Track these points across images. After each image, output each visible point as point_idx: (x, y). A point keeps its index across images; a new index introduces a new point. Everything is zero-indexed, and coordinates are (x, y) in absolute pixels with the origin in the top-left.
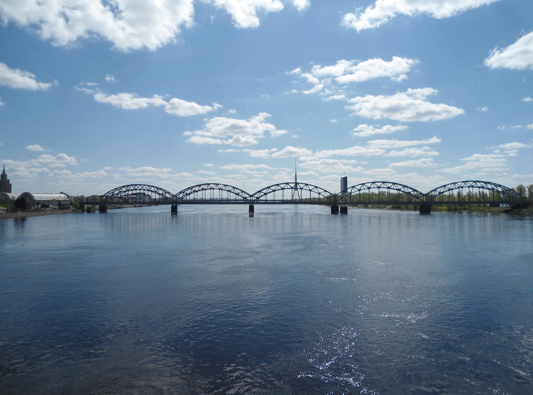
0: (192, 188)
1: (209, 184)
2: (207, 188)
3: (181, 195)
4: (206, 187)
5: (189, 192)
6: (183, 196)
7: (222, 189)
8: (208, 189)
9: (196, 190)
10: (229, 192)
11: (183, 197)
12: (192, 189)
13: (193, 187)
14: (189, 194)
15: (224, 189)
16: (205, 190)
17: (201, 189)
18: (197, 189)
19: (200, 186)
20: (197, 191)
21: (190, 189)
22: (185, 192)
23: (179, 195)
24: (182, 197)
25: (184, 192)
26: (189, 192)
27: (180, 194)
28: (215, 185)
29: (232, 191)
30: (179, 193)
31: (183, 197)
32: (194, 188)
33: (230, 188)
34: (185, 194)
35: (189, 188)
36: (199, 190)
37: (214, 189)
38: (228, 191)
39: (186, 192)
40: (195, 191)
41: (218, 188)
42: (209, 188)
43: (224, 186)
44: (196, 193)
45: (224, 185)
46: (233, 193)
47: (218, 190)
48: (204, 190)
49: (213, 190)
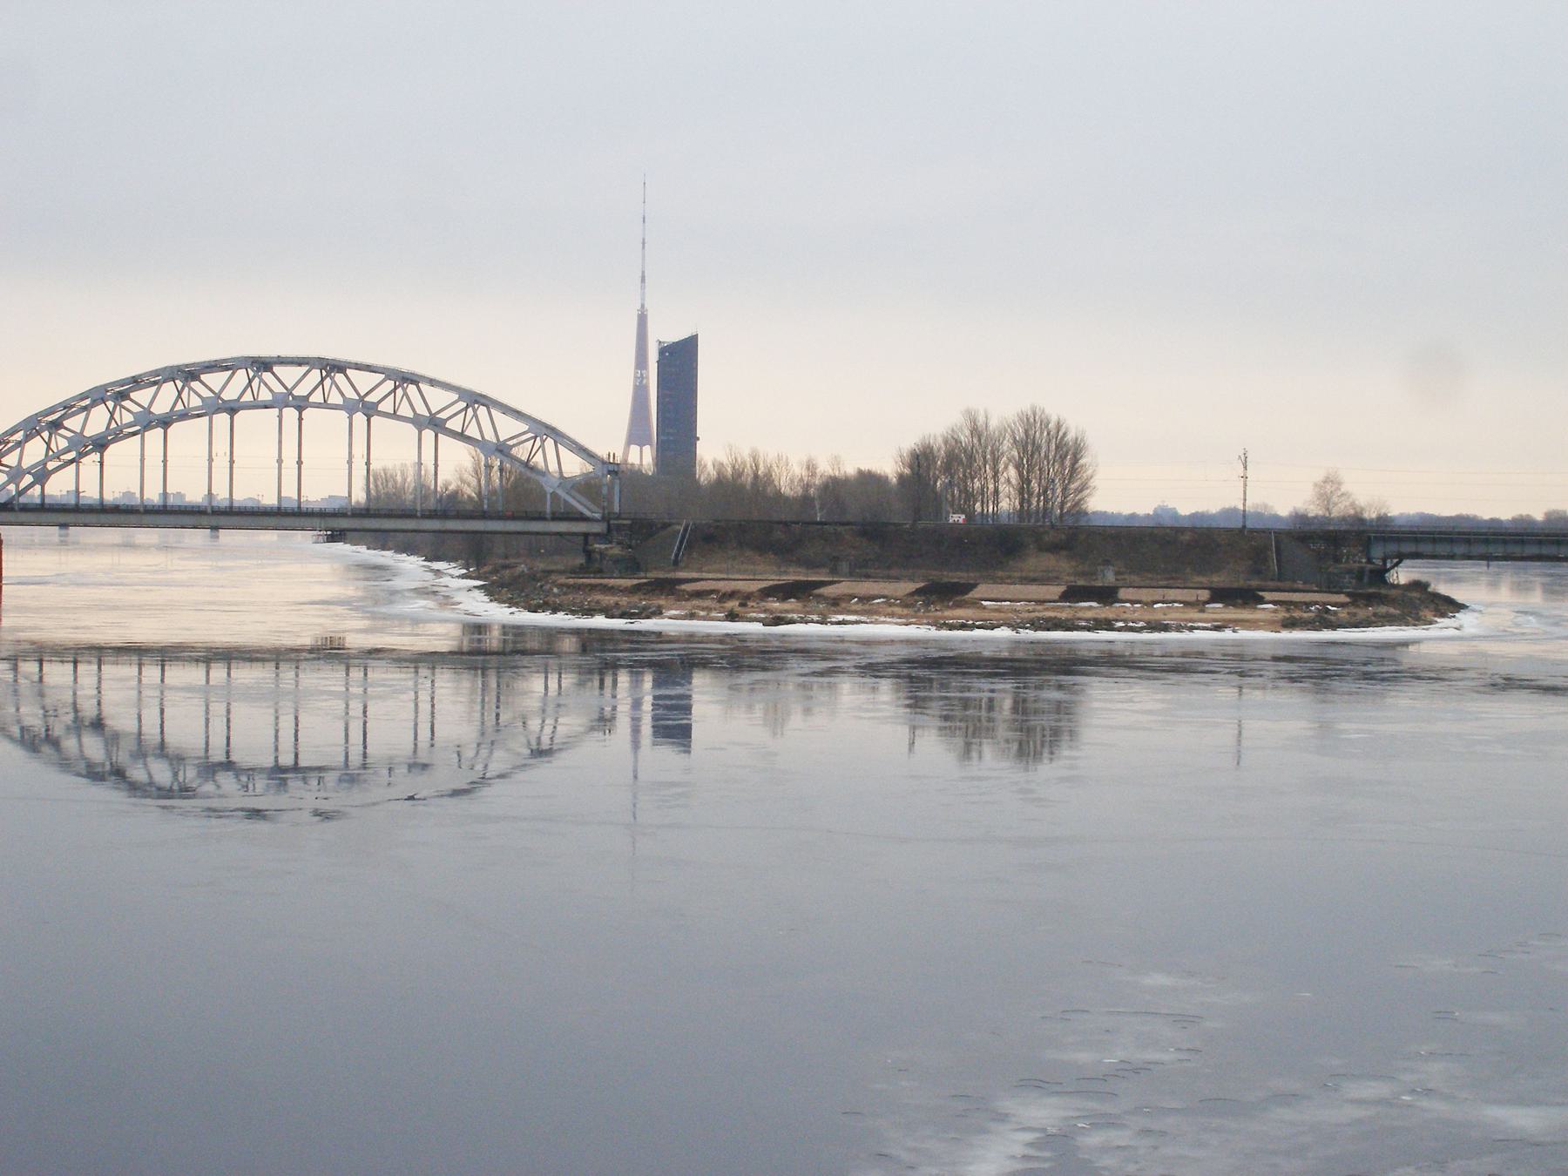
0: (123, 396)
1: (264, 365)
2: (248, 397)
3: (35, 451)
4: (235, 386)
5: (98, 421)
6: (48, 458)
7: (370, 410)
8: (257, 405)
9: (161, 407)
10: (428, 434)
11: (51, 465)
12: (126, 403)
13: (137, 382)
14: (101, 444)
15: (386, 406)
16: (232, 409)
17: (195, 402)
18: (165, 399)
19: (190, 374)
20: (165, 422)
21: (110, 404)
22: (66, 423)
23: (19, 444)
24: (44, 463)
25: (56, 426)
26: (98, 421)
27: (28, 438)
28: (315, 375)
29: (449, 425)
30: (13, 431)
31: (51, 465)
32: (142, 396)
33: (438, 399)
34: (63, 444)
35: (98, 396)
36: (185, 416)
37: (301, 404)
38: (419, 422)
39: (74, 423)
40: (148, 421)
41: (335, 399)
42: (265, 396)
43: (390, 385)
44: (160, 431)
45: (389, 373)
46: (461, 436)
47: (344, 414)
48: (218, 410)
49: (300, 409)
